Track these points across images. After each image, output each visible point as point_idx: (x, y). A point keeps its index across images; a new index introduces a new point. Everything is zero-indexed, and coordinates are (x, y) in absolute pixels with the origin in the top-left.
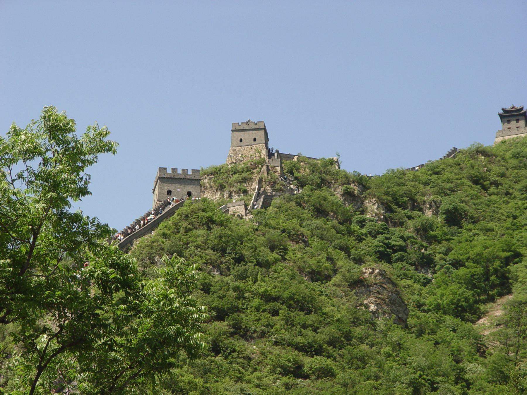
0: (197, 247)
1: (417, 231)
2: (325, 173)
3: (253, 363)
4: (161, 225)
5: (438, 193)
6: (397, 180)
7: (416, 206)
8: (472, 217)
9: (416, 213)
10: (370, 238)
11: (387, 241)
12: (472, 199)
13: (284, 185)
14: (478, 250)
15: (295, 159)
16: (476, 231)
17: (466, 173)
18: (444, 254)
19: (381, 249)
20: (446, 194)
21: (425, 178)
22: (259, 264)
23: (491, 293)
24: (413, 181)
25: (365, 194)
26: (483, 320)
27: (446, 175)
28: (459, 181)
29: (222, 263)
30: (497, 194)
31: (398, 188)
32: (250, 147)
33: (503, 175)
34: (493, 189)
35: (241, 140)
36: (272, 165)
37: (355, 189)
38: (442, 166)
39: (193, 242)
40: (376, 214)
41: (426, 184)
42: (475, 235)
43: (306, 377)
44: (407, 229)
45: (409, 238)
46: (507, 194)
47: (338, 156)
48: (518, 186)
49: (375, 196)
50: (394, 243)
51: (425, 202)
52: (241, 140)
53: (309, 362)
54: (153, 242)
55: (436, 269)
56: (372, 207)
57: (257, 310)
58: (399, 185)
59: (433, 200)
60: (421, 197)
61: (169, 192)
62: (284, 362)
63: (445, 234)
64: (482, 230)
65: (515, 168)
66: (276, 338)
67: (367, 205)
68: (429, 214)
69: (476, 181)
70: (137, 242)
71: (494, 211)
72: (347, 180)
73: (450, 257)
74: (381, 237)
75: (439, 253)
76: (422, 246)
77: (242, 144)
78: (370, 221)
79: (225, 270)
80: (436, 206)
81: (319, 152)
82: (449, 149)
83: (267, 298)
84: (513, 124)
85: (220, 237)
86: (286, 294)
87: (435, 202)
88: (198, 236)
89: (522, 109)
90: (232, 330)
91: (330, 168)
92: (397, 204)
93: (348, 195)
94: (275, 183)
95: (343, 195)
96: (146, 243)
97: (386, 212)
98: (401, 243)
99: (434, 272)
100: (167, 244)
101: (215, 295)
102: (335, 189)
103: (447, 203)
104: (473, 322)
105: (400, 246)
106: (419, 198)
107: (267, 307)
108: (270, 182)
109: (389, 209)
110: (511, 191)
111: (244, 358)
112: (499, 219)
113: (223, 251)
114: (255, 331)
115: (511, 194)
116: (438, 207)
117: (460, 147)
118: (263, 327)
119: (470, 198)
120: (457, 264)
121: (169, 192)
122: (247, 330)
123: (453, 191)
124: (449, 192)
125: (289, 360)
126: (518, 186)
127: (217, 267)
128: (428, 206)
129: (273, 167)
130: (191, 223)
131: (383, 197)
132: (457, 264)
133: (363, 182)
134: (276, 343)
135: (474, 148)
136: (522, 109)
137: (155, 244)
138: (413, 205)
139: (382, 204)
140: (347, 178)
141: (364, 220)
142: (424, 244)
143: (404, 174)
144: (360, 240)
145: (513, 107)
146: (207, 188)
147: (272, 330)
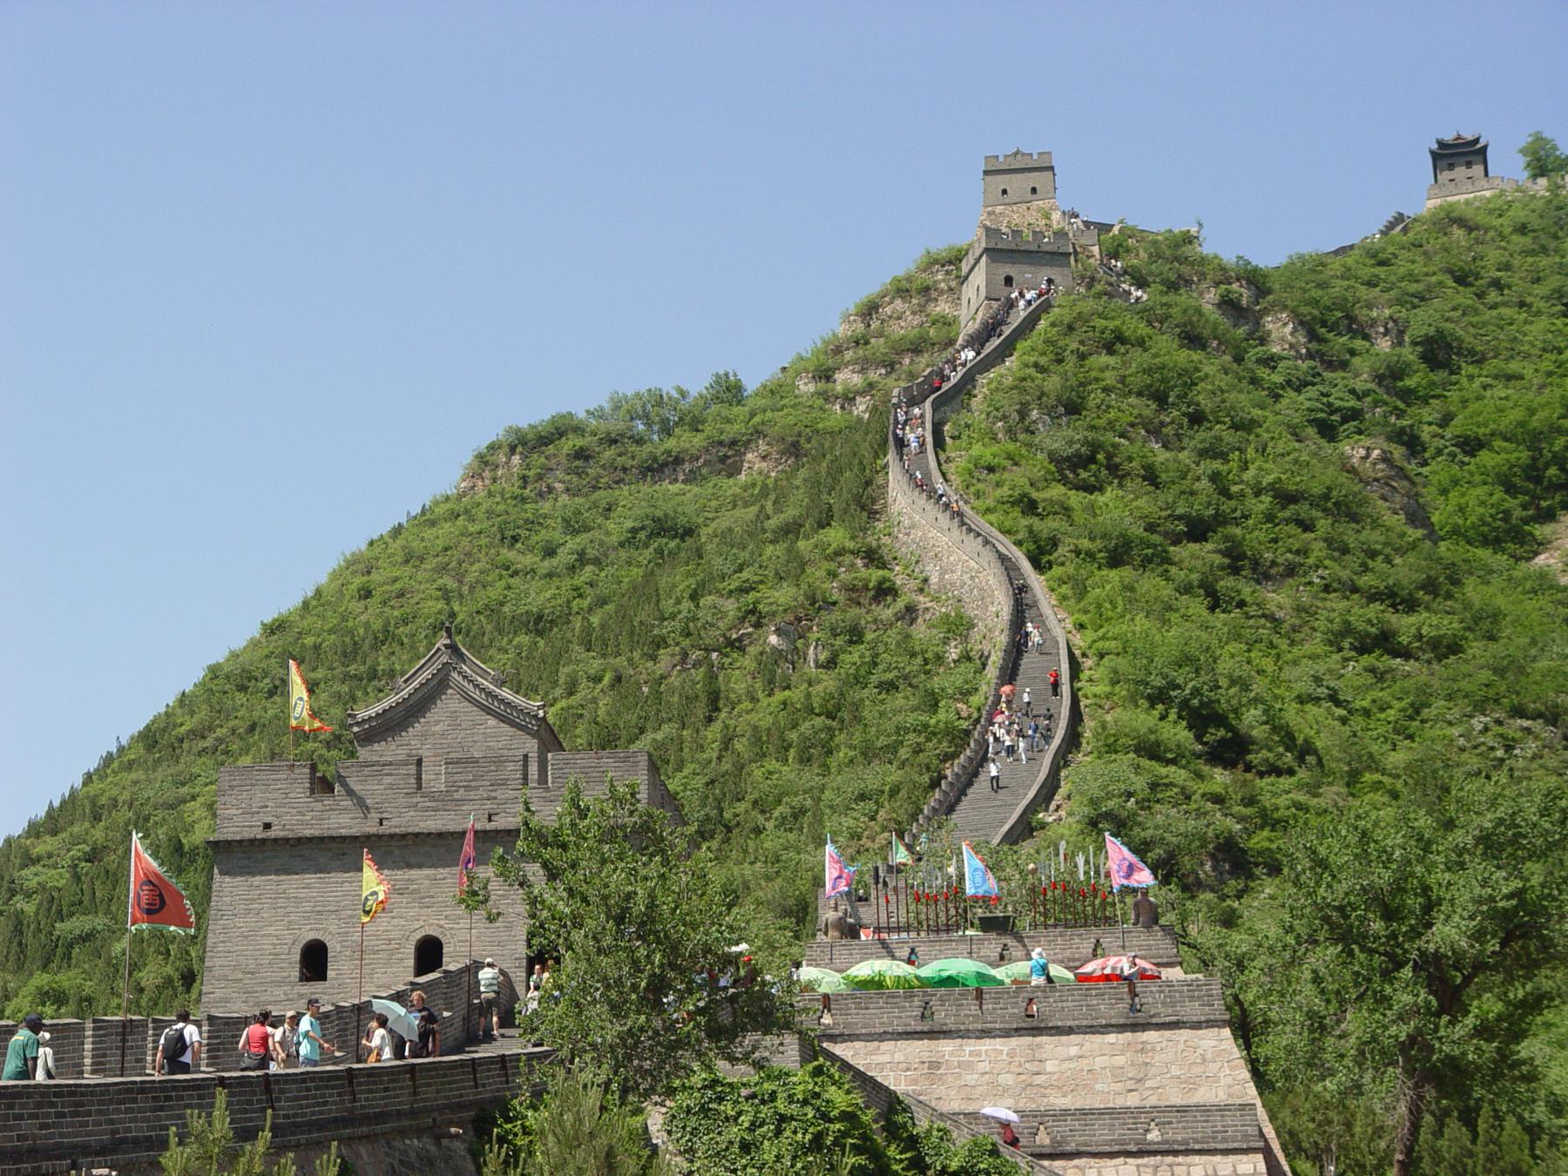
0: (1106, 390)
1: (1379, 379)
2: (1176, 261)
3: (1286, 626)
4: (1022, 346)
5: (1399, 302)
6: (1312, 277)
7: (1362, 332)
8: (1472, 352)
9: (1359, 344)
10: (1293, 394)
11: (1325, 400)
12: (1464, 314)
13: (1111, 284)
14: (1516, 415)
15: (1116, 230)
16: (1489, 381)
17: (1439, 261)
18: (1440, 426)
19: (1320, 415)
20: (1415, 307)
21: (1367, 272)
22: (1236, 427)
23: (1544, 504)
24: (1343, 277)
25: (1264, 304)
26: (1542, 556)
27: (1402, 266)
28: (1433, 279)
29: (1162, 424)
30: (1504, 304)
31: (1320, 292)
32: (1024, 206)
33: (1507, 267)
34: (1493, 296)
35: (1004, 192)
36: (1082, 242)
37: (1244, 294)
38: (1391, 249)
39: (1097, 380)
40: (1292, 346)
41: (1370, 284)
42: (1485, 387)
43: (1406, 654)
44: (1357, 376)
45: (1367, 393)
46: (1522, 304)
47: (1200, 225)
48: (1542, 290)
49: (1285, 307)
50: (1338, 403)
51: (1373, 323)
52: (1004, 192)
53: (1406, 625)
54: (1024, 379)
55: (1427, 455)
56: (1281, 331)
57: (1270, 518)
58: (1319, 286)
59: (1391, 318)
60: (1365, 311)
61: (1009, 281)
62: (1361, 626)
63: (1432, 384)
64: (1496, 377)
65: (1528, 253)
66: (1322, 578)
67: (1270, 326)
68: (1384, 345)
69: (1462, 279)
70: (982, 380)
71: (1515, 339)
72: (1224, 276)
73: (1456, 428)
74: (1311, 392)
75: (1430, 424)
76: (1396, 408)
77: (1007, 199)
78: (1282, 358)
79: (1173, 439)
80: (1398, 332)
81: (1157, 216)
82: (1389, 216)
83: (1286, 498)
84: (1460, 172)
85: (1149, 371)
86: (1317, 490)
87: (1395, 321)
88: (1102, 370)
89: (1477, 141)
90: (1227, 561)
91: (1186, 250)
92: (1324, 324)
93: (1228, 304)
94: (1093, 279)
95: (1219, 306)
96: (1009, 381)
97: (1310, 341)
98: (1353, 403)
99: (1425, 464)
100: (1053, 383)
101: (1175, 490)
102: (1201, 294)
103: (1422, 322)
104: (1529, 559)
105: (1352, 409)
106: (1361, 314)
107: (1287, 514)
108: (1083, 278)
109: (1313, 336)
110: (1529, 300)
111: (1264, 616)
112: (1527, 356)
113: (1161, 400)
114: (1274, 563)
115: (1530, 306)
116: (1401, 333)
117: (1410, 212)
118: (1289, 555)
119: (1459, 313)
120: (1471, 445)
121: (1009, 281)
122: (1256, 564)
123: (1423, 299)
124: (1416, 301)
125: (1369, 622)
126: (1542, 290)
127: (1155, 431)
128: (1382, 330)
129: (1084, 247)
130: (1082, 343)
131: (1304, 310)
132: (1471, 445)
133: (1256, 280)
134: (1327, 589)
135: (1442, 215)
136: (1477, 141)
137: (1029, 383)
138: (1350, 326)
139: (1302, 323)
140: (1223, 269)
141: (1272, 358)
142: (1402, 405)
143: (1323, 264)
144: (1277, 397)
145: (1459, 138)
146: (942, 292)
147: (1311, 561)
